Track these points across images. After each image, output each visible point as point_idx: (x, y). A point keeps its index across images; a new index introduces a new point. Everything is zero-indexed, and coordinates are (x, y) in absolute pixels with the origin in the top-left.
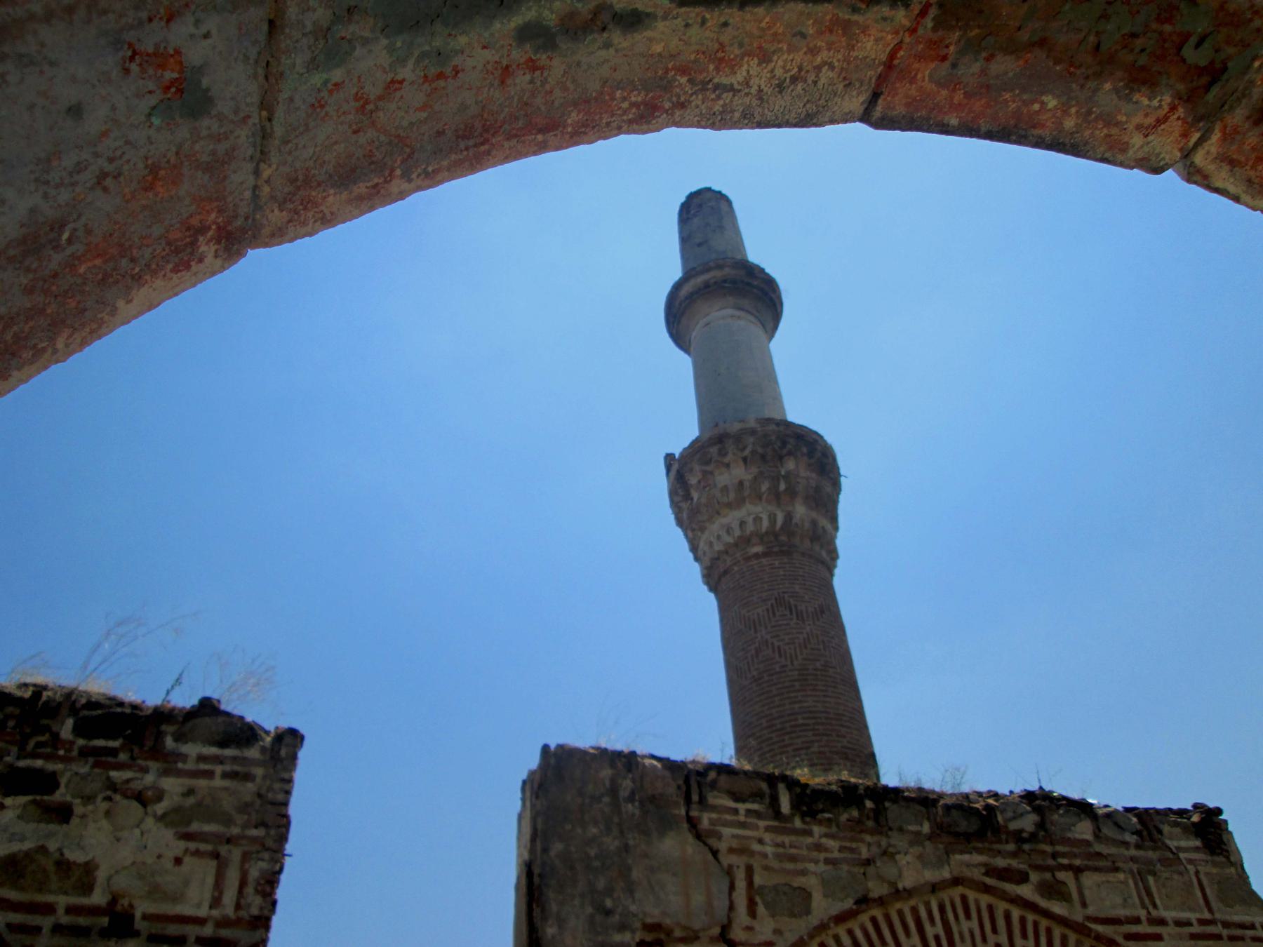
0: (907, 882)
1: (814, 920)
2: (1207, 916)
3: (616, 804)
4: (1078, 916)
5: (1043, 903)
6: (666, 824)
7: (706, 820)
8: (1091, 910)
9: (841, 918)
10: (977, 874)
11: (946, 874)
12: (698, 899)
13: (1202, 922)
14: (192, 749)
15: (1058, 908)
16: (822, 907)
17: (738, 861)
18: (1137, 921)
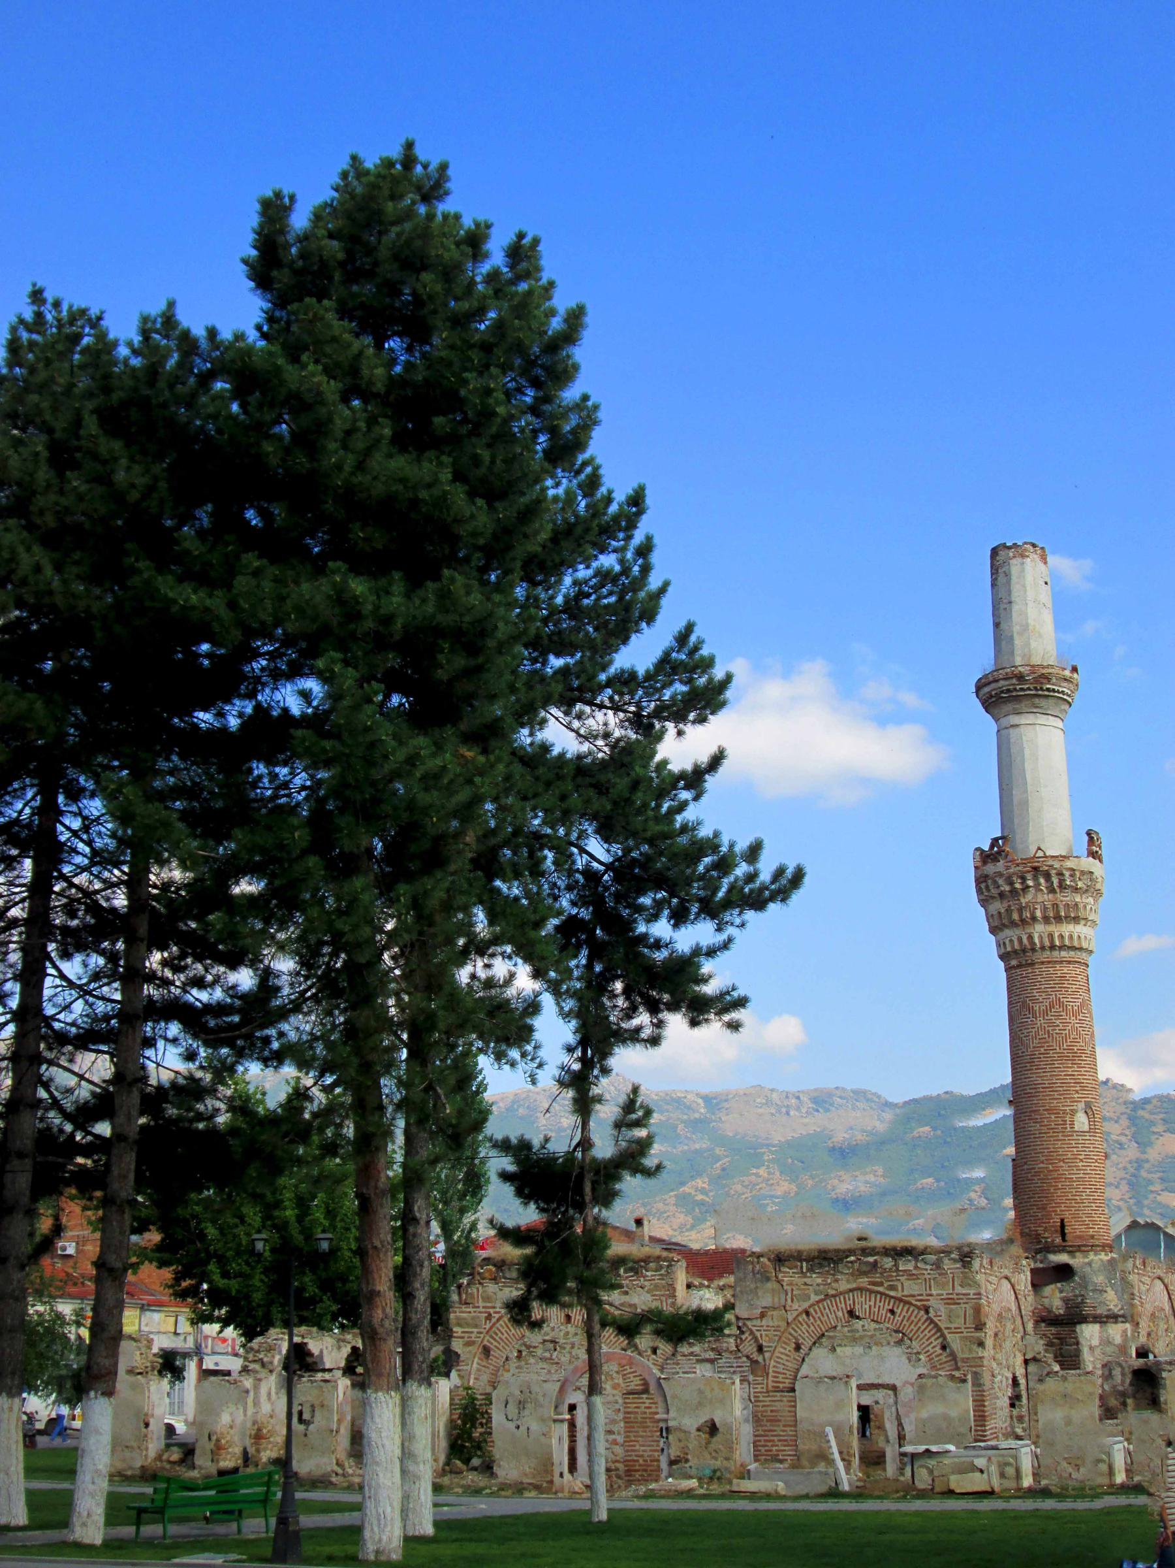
0: (841, 1289)
1: (811, 1302)
3: (754, 1275)
4: (899, 1295)
5: (888, 1292)
6: (768, 1279)
7: (780, 1276)
8: (905, 1293)
9: (818, 1302)
10: (865, 1285)
11: (854, 1285)
12: (776, 1300)
14: (649, 1274)
15: (892, 1293)
16: (814, 1298)
17: (789, 1288)
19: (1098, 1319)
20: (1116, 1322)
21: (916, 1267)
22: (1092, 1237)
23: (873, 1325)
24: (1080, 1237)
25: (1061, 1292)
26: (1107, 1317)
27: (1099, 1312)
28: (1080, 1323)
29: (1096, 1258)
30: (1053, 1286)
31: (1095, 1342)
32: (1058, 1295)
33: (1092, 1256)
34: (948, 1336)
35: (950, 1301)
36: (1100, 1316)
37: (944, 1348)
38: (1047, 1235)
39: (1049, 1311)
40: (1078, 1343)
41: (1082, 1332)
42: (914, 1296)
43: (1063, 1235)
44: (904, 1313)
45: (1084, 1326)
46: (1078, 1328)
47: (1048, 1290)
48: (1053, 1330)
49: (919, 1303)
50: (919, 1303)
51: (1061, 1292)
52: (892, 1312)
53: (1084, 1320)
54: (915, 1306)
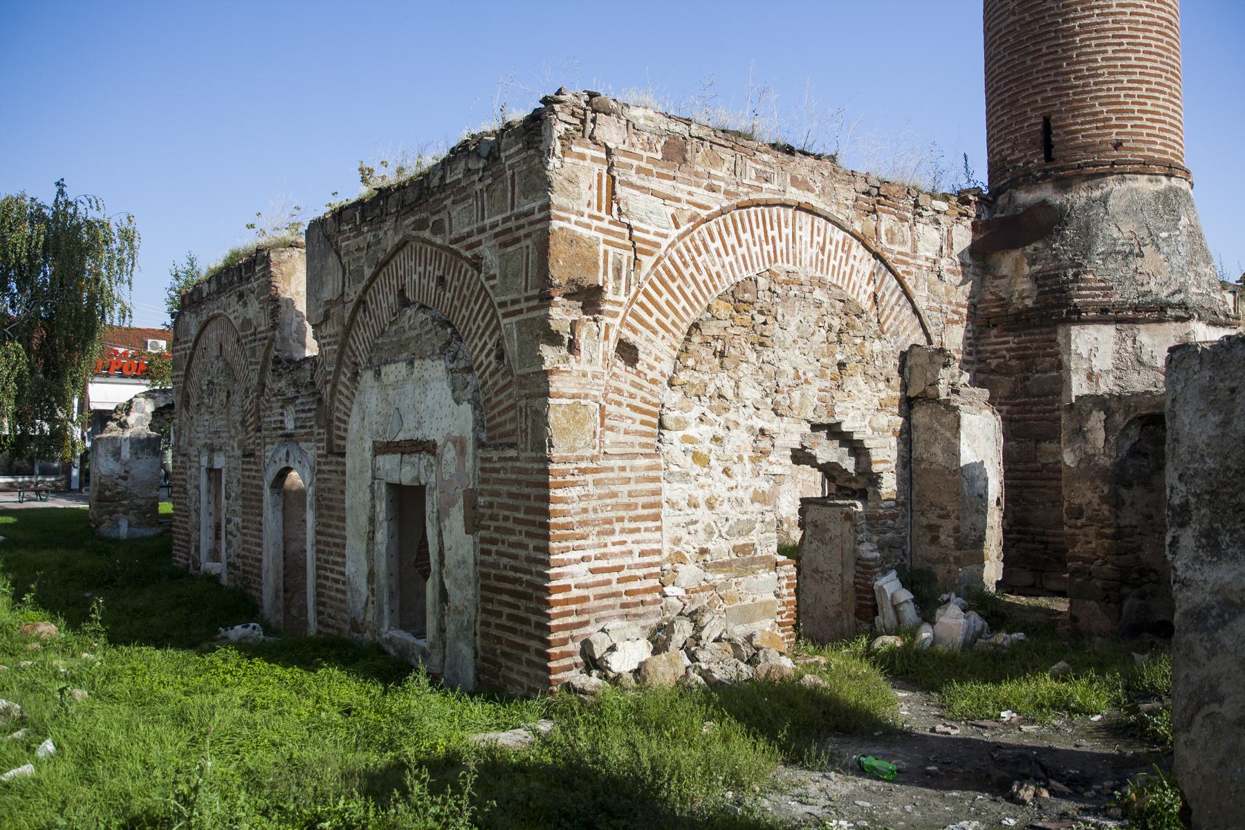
2: (509, 213)
8: (454, 235)
13: (505, 220)
18: (470, 235)
19: (1105, 315)
20: (1160, 321)
21: (468, 172)
22: (1118, 145)
23: (422, 316)
24: (1085, 147)
25: (1032, 262)
26: (1136, 308)
27: (1116, 298)
28: (1069, 321)
29: (1124, 186)
30: (1016, 254)
31: (1104, 362)
32: (1027, 270)
33: (1111, 184)
34: (504, 322)
35: (506, 238)
36: (1121, 307)
37: (500, 357)
38: (1017, 155)
39: (1003, 303)
40: (1060, 366)
41: (1068, 336)
42: (462, 238)
43: (1048, 147)
44: (455, 283)
45: (1075, 330)
46: (1061, 330)
47: (1007, 262)
48: (1012, 340)
49: (468, 254)
50: (468, 254)
51: (1032, 262)
52: (441, 281)
53: (1076, 317)
54: (466, 259)
